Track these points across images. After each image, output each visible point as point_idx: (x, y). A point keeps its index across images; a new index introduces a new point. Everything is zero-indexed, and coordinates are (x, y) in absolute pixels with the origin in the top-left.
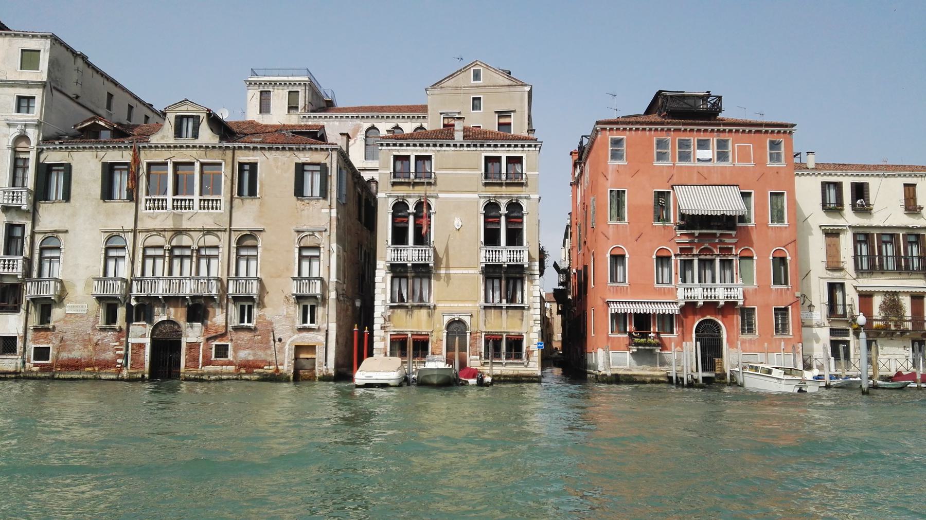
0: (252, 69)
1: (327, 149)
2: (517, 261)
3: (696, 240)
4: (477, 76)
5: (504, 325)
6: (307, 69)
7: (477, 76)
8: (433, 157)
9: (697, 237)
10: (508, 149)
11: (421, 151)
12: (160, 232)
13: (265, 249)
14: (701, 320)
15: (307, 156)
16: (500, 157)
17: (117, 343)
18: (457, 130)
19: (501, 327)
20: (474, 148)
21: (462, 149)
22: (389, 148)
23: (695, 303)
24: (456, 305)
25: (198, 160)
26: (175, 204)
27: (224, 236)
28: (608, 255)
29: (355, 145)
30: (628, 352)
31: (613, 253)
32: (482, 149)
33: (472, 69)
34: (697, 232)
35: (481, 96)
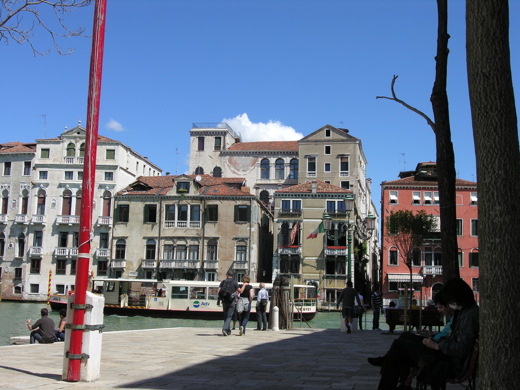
0: (193, 124)
1: (250, 198)
2: (342, 254)
3: (433, 244)
4: (328, 134)
5: (336, 285)
6: (226, 124)
7: (328, 134)
8: (301, 201)
9: (433, 242)
10: (338, 197)
11: (295, 198)
12: (172, 238)
13: (221, 247)
14: (435, 284)
15: (241, 201)
16: (335, 201)
17: (153, 291)
18: (313, 188)
19: (334, 286)
20: (322, 197)
21: (315, 197)
22: (280, 197)
23: (432, 276)
24: (312, 275)
25: (189, 204)
26: (179, 225)
27: (201, 241)
28: (389, 250)
29: (255, 169)
30: (398, 299)
31: (391, 250)
32: (326, 197)
33: (325, 129)
34: (433, 240)
35: (331, 146)
